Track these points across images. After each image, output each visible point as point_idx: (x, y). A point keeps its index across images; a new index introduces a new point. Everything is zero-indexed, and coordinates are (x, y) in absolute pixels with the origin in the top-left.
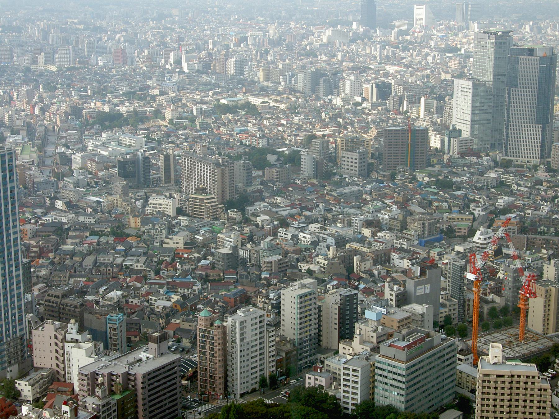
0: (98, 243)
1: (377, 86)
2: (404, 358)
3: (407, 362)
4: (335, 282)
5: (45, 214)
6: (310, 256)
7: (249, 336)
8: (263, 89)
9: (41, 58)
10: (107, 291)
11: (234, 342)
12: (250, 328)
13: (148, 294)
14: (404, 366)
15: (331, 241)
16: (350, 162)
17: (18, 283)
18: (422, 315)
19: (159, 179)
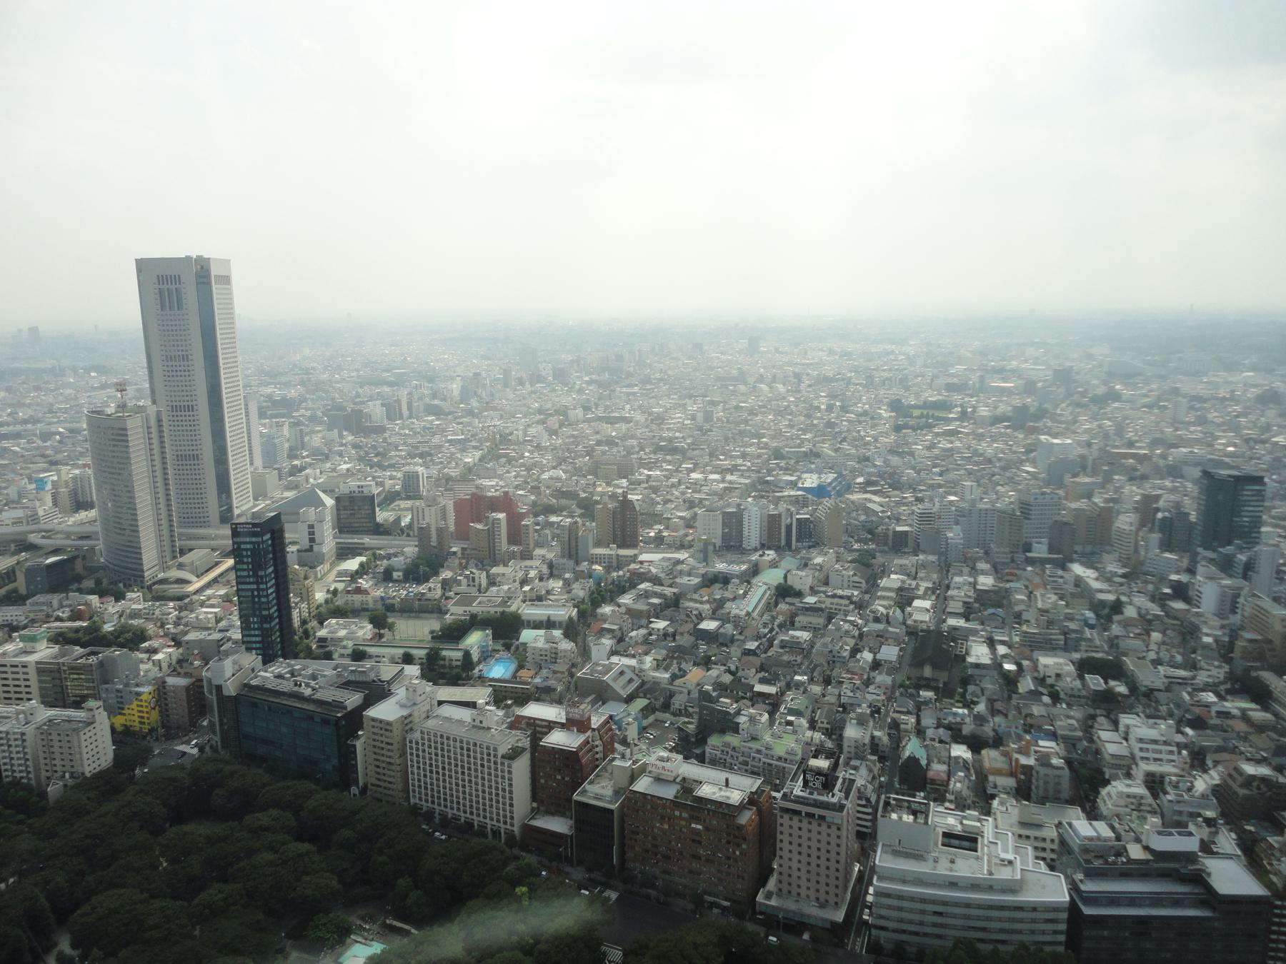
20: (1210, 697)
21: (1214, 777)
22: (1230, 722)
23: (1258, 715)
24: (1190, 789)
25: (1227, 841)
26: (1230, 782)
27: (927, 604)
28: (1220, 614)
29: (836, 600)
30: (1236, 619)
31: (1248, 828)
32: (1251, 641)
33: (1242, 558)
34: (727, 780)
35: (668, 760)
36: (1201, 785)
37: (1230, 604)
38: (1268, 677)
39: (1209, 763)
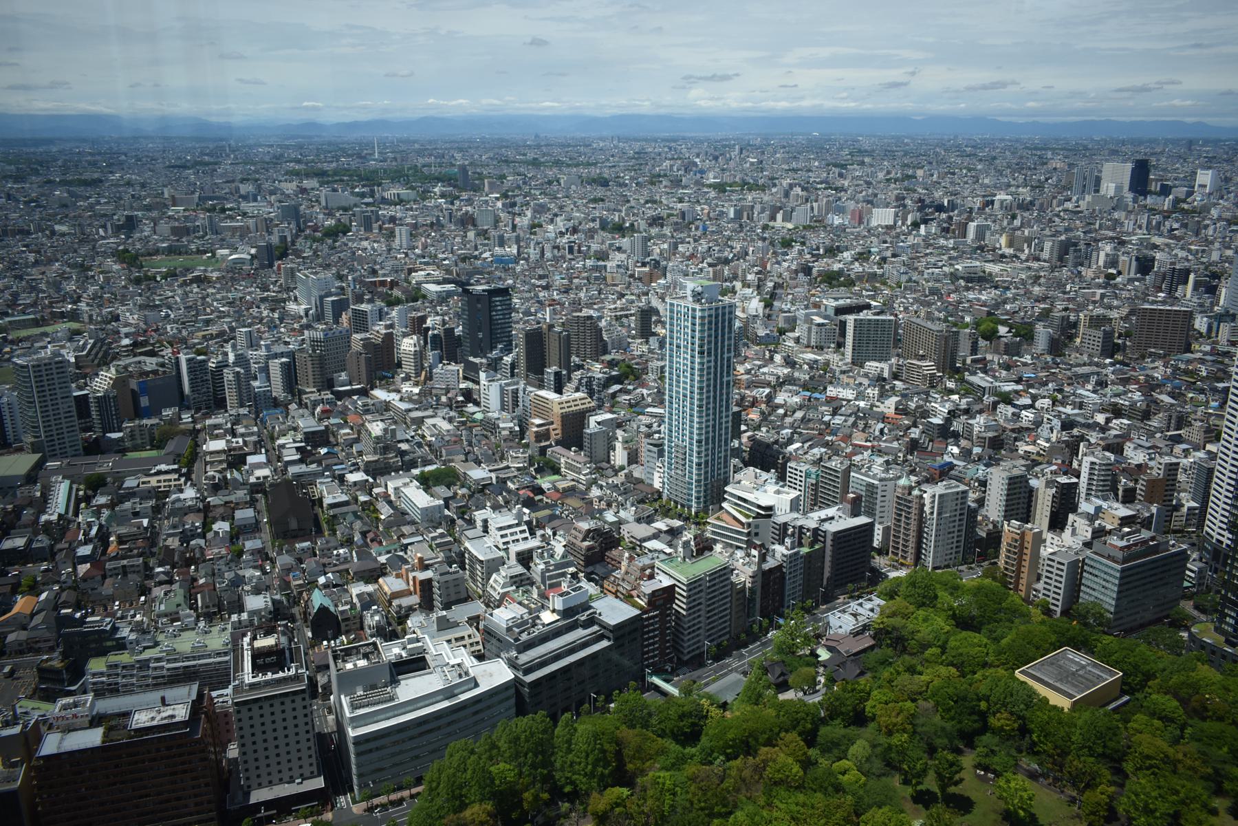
1: (1137, 259)
8: (1003, 256)
14: (1119, 567)
27: (261, 458)
29: (162, 477)
32: (539, 426)
34: (163, 699)
35: (75, 705)
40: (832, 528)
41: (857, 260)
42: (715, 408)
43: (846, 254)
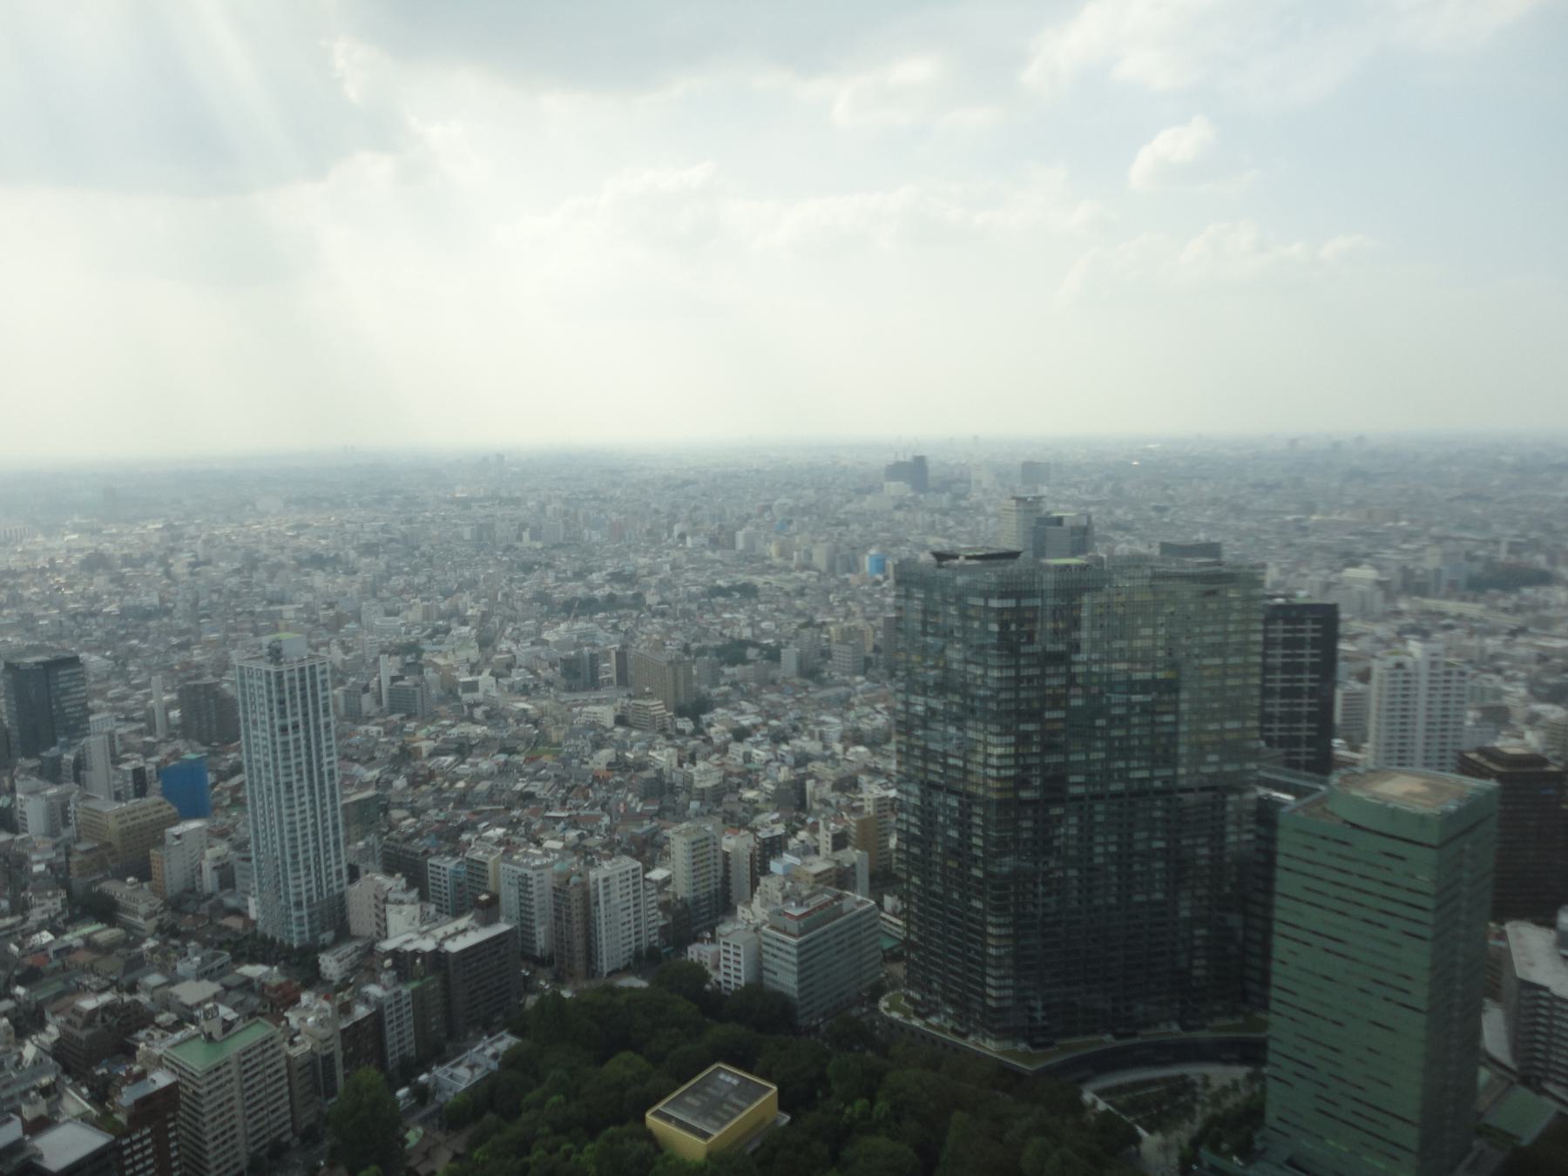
0: (506, 763)
2: (796, 931)
3: (801, 935)
4: (776, 816)
5: (453, 726)
6: (757, 782)
7: (616, 899)
8: (771, 567)
9: (526, 535)
10: (486, 829)
11: (597, 903)
12: (618, 886)
13: (543, 830)
15: (790, 759)
16: (842, 654)
17: (335, 827)
18: (853, 866)
19: (610, 681)
20: (46, 937)
21: (52, 1032)
22: (72, 957)
23: (103, 933)
24: (19, 1062)
25: (75, 1101)
26: (71, 1029)
28: (53, 832)
30: (66, 833)
31: (99, 1072)
32: (87, 852)
33: (69, 757)
36: (29, 1051)
37: (59, 815)
38: (113, 888)
39: (48, 1016)
40: (454, 946)
41: (608, 581)
42: (313, 801)
43: (594, 576)
